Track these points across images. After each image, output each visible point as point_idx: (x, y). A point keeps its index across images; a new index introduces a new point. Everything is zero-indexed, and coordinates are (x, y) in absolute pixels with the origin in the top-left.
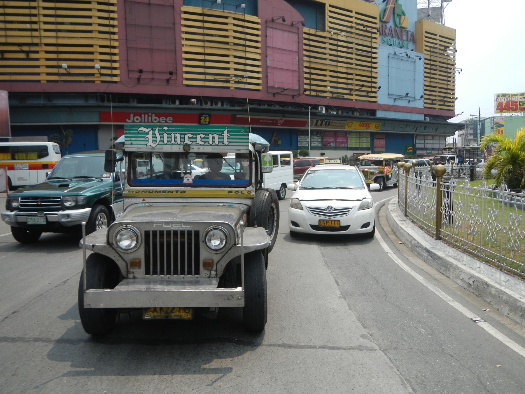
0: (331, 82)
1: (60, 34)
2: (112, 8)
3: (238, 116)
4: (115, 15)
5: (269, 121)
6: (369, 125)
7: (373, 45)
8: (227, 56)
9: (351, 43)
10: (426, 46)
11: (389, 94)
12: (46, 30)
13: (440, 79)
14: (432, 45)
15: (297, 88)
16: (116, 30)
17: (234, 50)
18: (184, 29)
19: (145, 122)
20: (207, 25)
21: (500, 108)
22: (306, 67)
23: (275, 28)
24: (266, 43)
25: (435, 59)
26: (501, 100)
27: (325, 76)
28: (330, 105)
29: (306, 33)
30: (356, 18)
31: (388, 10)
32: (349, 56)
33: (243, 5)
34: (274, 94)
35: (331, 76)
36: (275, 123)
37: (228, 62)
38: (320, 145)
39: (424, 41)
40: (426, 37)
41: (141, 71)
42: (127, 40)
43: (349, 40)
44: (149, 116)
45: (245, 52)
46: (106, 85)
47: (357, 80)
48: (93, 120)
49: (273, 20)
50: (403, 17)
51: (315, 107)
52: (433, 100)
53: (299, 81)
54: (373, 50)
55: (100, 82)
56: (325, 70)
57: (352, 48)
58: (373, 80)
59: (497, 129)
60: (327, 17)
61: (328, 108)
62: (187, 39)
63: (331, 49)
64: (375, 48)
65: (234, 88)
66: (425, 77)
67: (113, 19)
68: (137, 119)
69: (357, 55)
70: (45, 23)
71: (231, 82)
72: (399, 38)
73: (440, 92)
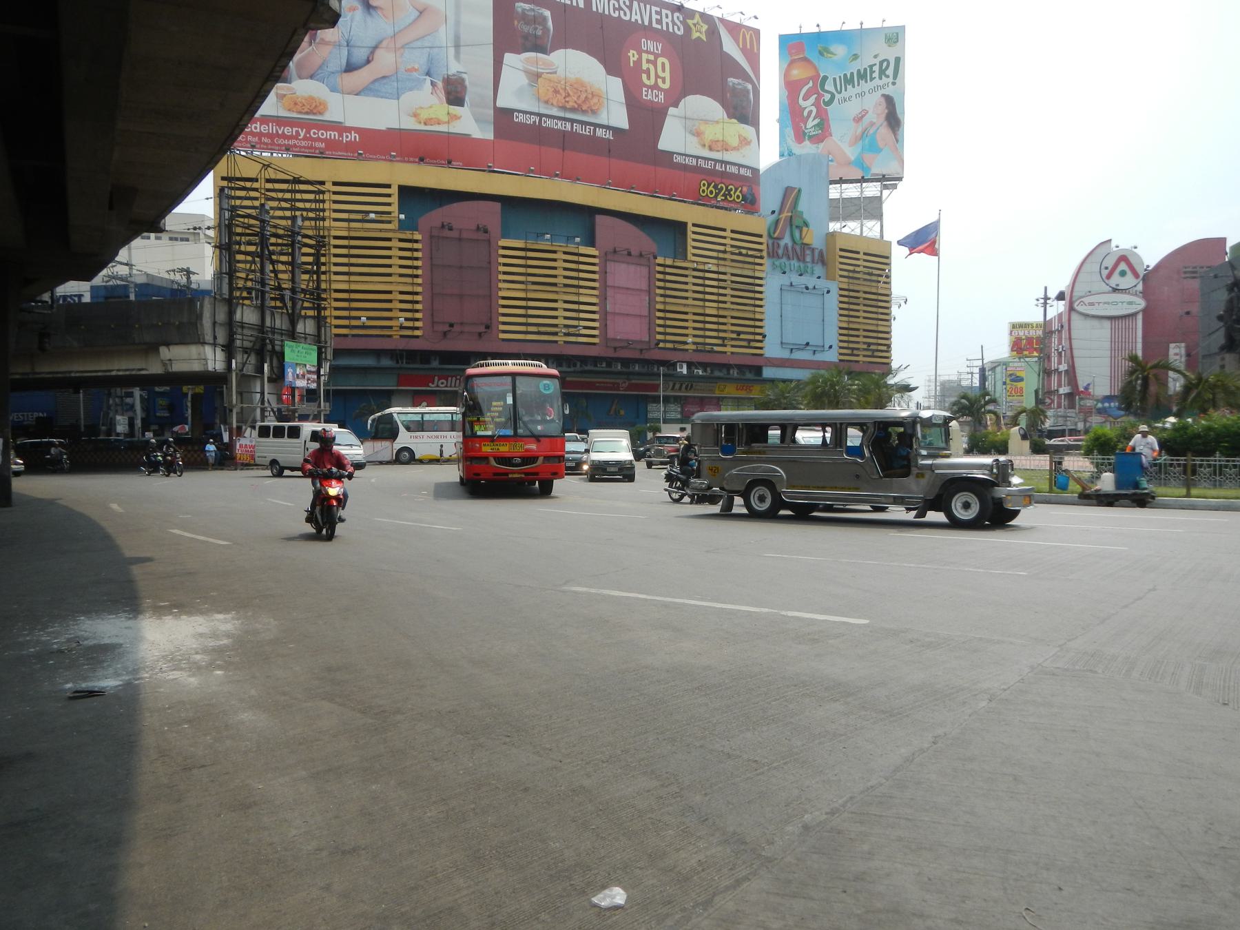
0: (695, 329)
1: (353, 278)
2: (416, 246)
3: (568, 379)
4: (419, 254)
5: (609, 385)
6: (751, 388)
7: (757, 274)
8: (556, 301)
9: (724, 274)
10: (841, 270)
11: (782, 343)
12: (336, 273)
13: (865, 318)
14: (851, 268)
15: (647, 339)
16: (419, 272)
17: (564, 292)
18: (501, 269)
19: (451, 386)
20: (530, 262)
21: (1018, 347)
22: (660, 310)
23: (617, 261)
24: (606, 282)
25: (856, 288)
26: (1018, 335)
27: (687, 321)
28: (693, 360)
29: (659, 265)
30: (732, 239)
31: (782, 222)
32: (721, 291)
33: (578, 240)
34: (615, 349)
35: (695, 321)
36: (616, 386)
37: (556, 309)
38: (679, 416)
39: (837, 264)
40: (841, 257)
41: (451, 325)
42: (432, 284)
43: (722, 269)
44: (456, 379)
45: (578, 294)
46: (407, 339)
47: (733, 325)
48: (389, 384)
49: (615, 252)
50: (805, 229)
51: (672, 365)
52: (853, 349)
53: (649, 329)
54: (758, 282)
55: (398, 337)
56: (686, 313)
57: (725, 281)
58: (758, 323)
59: (1012, 385)
60: (689, 241)
61: (690, 365)
62: (505, 281)
63: (694, 284)
64: (761, 278)
65: (562, 342)
66: (841, 315)
67: (416, 259)
68: (442, 383)
69: (732, 289)
70: (336, 264)
71: (559, 334)
72: (799, 260)
73: (865, 337)
